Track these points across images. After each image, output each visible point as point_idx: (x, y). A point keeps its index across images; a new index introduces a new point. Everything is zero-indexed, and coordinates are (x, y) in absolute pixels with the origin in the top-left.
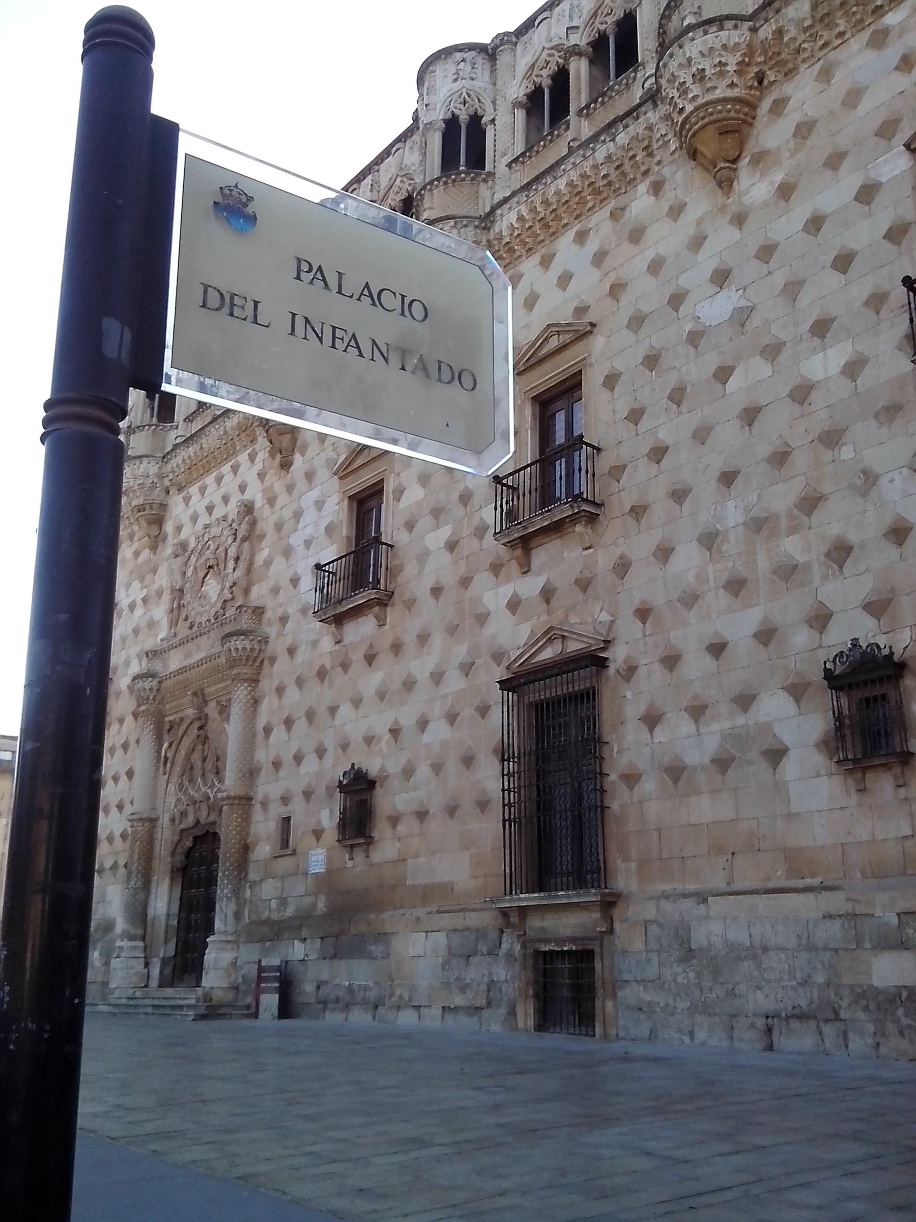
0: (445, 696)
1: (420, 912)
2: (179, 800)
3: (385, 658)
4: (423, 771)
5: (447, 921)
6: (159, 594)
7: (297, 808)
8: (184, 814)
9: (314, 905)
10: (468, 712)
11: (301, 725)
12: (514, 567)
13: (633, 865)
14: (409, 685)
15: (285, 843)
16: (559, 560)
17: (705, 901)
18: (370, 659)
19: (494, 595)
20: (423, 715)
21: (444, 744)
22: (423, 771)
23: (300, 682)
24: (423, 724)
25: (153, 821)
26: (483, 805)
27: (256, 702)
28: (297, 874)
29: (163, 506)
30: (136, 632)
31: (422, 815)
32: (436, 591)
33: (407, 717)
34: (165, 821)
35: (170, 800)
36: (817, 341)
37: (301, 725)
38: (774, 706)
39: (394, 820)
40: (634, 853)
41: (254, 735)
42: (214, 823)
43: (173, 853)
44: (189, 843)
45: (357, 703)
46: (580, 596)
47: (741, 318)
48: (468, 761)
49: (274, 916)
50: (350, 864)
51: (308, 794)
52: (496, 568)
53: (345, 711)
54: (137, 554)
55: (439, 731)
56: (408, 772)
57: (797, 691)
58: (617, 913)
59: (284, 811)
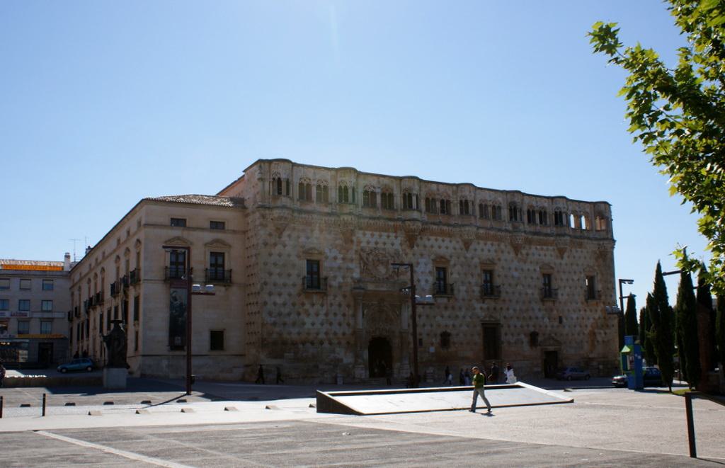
4: (461, 335)
19: (478, 305)
22: (461, 335)
24: (461, 326)
31: (462, 343)
38: (522, 336)
45: (442, 317)
47: (519, 278)
51: (428, 335)
52: (477, 300)
55: (464, 328)
56: (457, 335)
57: (525, 335)
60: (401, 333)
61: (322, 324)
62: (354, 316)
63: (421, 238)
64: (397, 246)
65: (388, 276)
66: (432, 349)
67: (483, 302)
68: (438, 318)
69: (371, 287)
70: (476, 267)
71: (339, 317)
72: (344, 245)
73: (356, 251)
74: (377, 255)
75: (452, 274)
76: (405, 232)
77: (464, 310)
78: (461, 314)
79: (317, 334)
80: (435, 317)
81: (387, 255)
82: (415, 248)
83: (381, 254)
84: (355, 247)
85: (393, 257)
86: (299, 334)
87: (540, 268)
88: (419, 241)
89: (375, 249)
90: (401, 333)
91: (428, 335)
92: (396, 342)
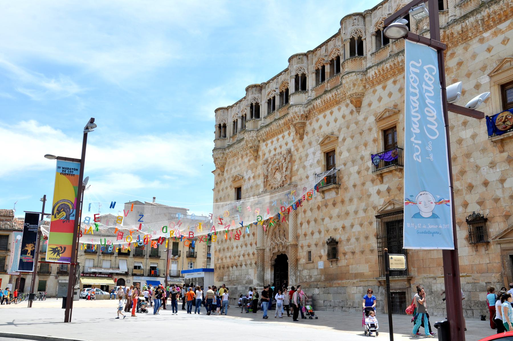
0: (358, 218)
1: (355, 281)
2: (272, 243)
3: (339, 205)
4: (353, 240)
5: (362, 284)
6: (259, 176)
7: (313, 249)
8: (274, 248)
9: (321, 278)
10: (366, 223)
11: (312, 223)
12: (378, 181)
13: (416, 269)
14: (347, 214)
15: (310, 259)
16: (391, 180)
17: (436, 279)
18: (334, 204)
19: (373, 189)
20: (352, 223)
21: (359, 232)
22: (353, 240)
23: (311, 210)
24: (352, 226)
25: (264, 250)
26: (372, 251)
27: (297, 215)
28: (314, 269)
29: (258, 146)
30: (251, 187)
31: (353, 253)
32: (355, 186)
33: (347, 224)
34: (267, 250)
35: (268, 244)
36: (463, 127)
37: (312, 223)
39: (345, 254)
40: (416, 266)
41: (297, 225)
42: (285, 252)
43: (271, 260)
45: (331, 218)
46: (398, 192)
48: (367, 238)
49: (308, 281)
50: (331, 266)
52: (373, 181)
53: (327, 220)
54: (249, 161)
55: (357, 228)
56: (348, 240)
58: (411, 282)
59: (309, 249)
61: (242, 247)
66: (321, 265)
67: (382, 182)
68: (327, 220)
70: (370, 130)
75: (341, 153)
77: (355, 200)
78: (351, 208)
79: (239, 256)
80: (323, 220)
86: (230, 257)
87: (490, 76)
91: (316, 245)
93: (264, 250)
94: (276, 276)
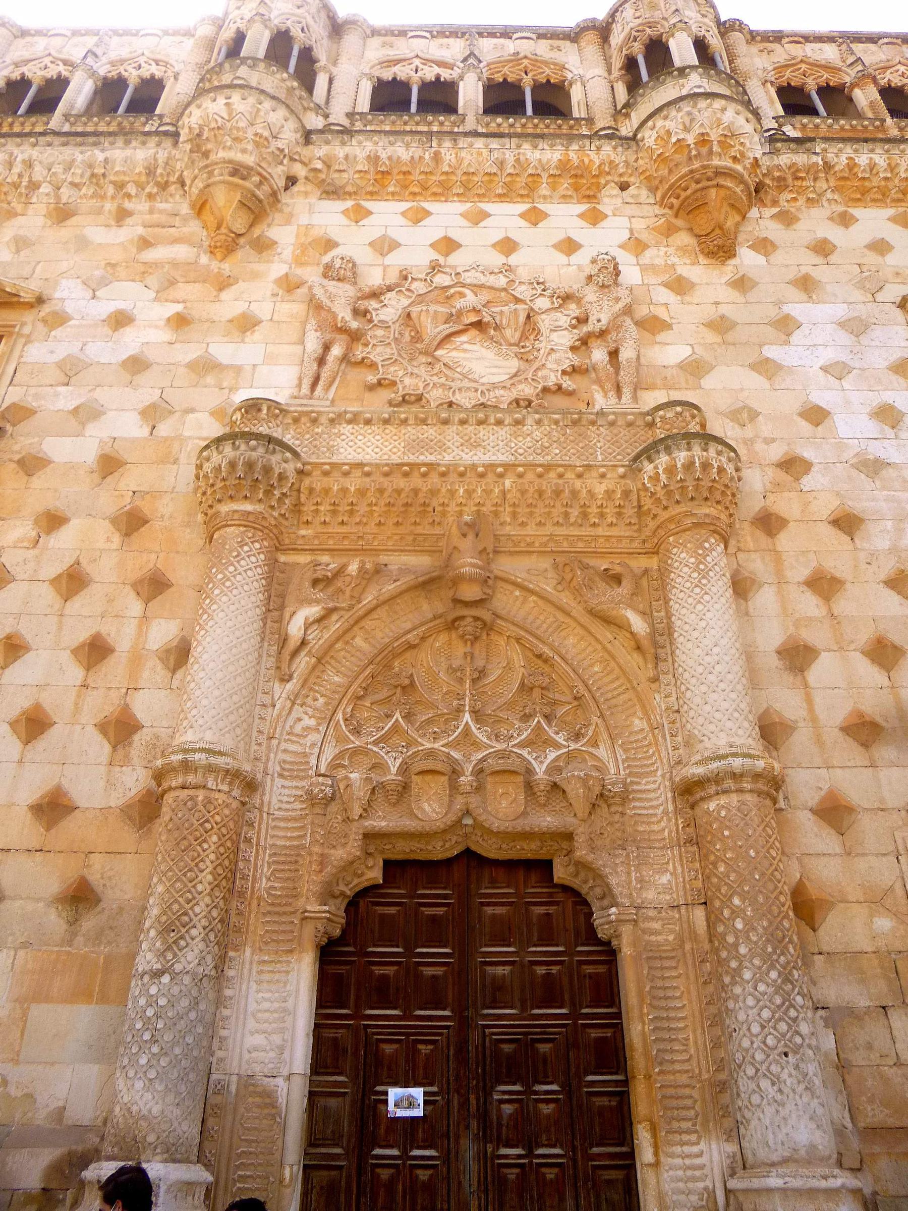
34: (279, 795)
43: (327, 894)
44: (375, 875)
60: (689, 792)
62: (180, 655)
63: (787, 219)
64: (608, 237)
65: (527, 390)
69: (363, 447)
71: (45, 672)
72: (204, 259)
73: (289, 285)
74: (445, 294)
76: (653, 190)
81: (522, 291)
82: (747, 258)
83: (477, 288)
84: (278, 269)
85: (567, 298)
88: (762, 221)
89: (435, 268)
90: (689, 792)
92: (645, 895)
93: (251, 786)
94: (345, 1055)
